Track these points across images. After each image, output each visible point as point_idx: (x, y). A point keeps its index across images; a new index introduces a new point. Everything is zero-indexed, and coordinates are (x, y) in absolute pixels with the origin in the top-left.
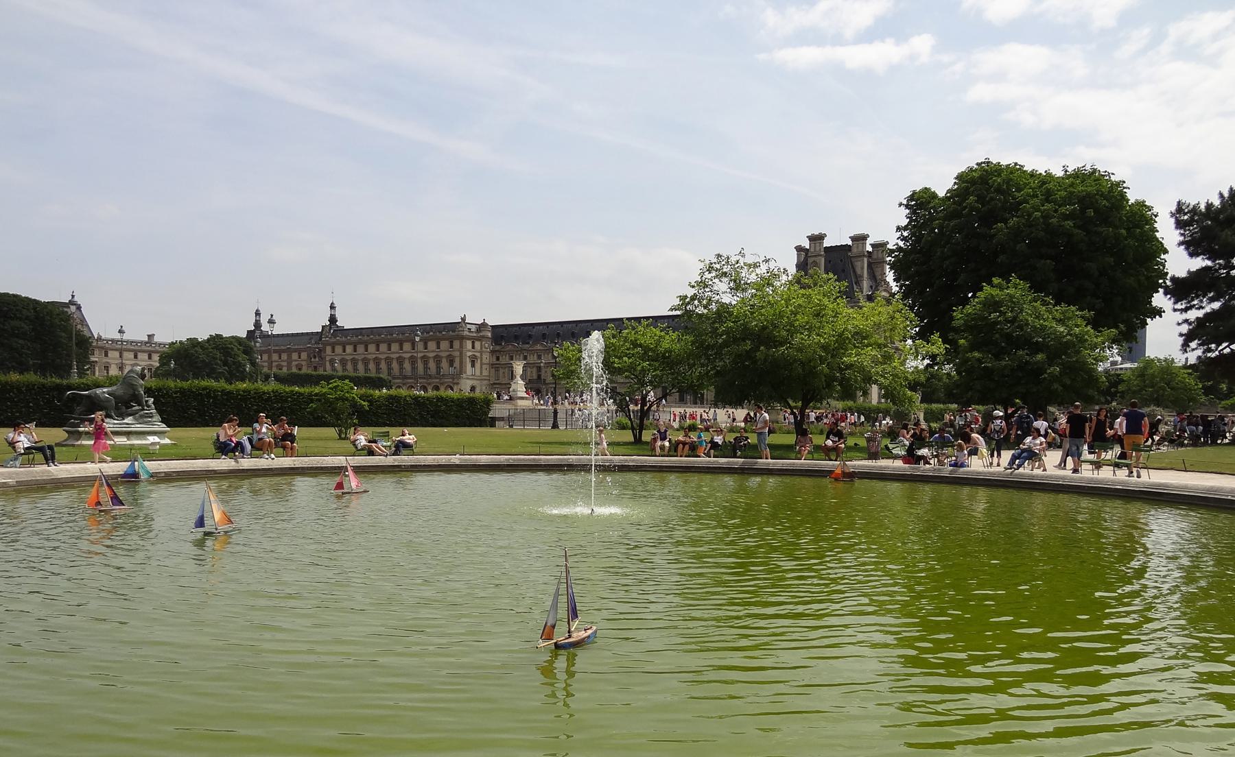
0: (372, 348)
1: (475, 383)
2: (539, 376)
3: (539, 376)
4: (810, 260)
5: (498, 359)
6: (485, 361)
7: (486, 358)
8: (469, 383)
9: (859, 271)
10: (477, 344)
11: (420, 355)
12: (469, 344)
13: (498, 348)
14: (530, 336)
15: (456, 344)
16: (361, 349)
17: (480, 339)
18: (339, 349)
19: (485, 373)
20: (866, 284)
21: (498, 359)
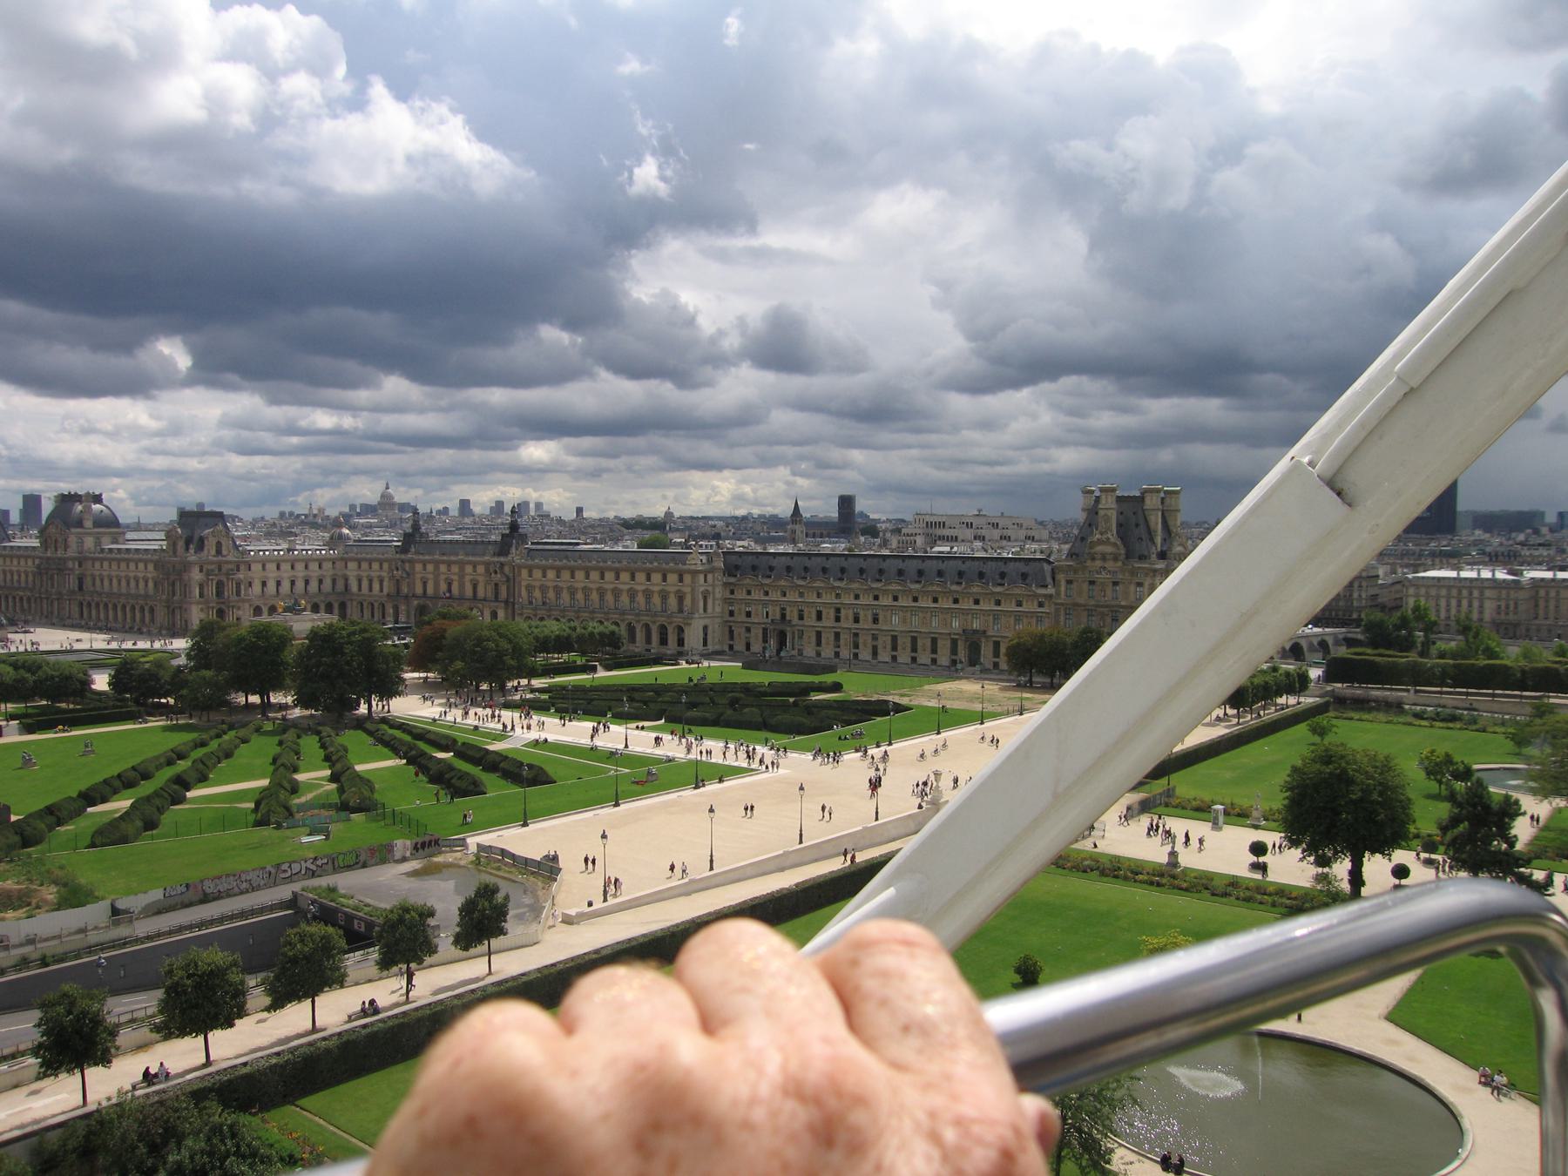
0: (580, 575)
1: (707, 621)
2: (783, 616)
3: (783, 616)
4: (1101, 513)
5: (732, 592)
6: (718, 595)
7: (719, 592)
8: (702, 623)
9: (1152, 525)
10: (710, 577)
11: (656, 589)
12: (702, 577)
13: (732, 580)
14: (771, 569)
15: (687, 578)
16: (566, 575)
17: (712, 571)
18: (537, 574)
19: (718, 609)
20: (1159, 540)
21: (732, 592)
